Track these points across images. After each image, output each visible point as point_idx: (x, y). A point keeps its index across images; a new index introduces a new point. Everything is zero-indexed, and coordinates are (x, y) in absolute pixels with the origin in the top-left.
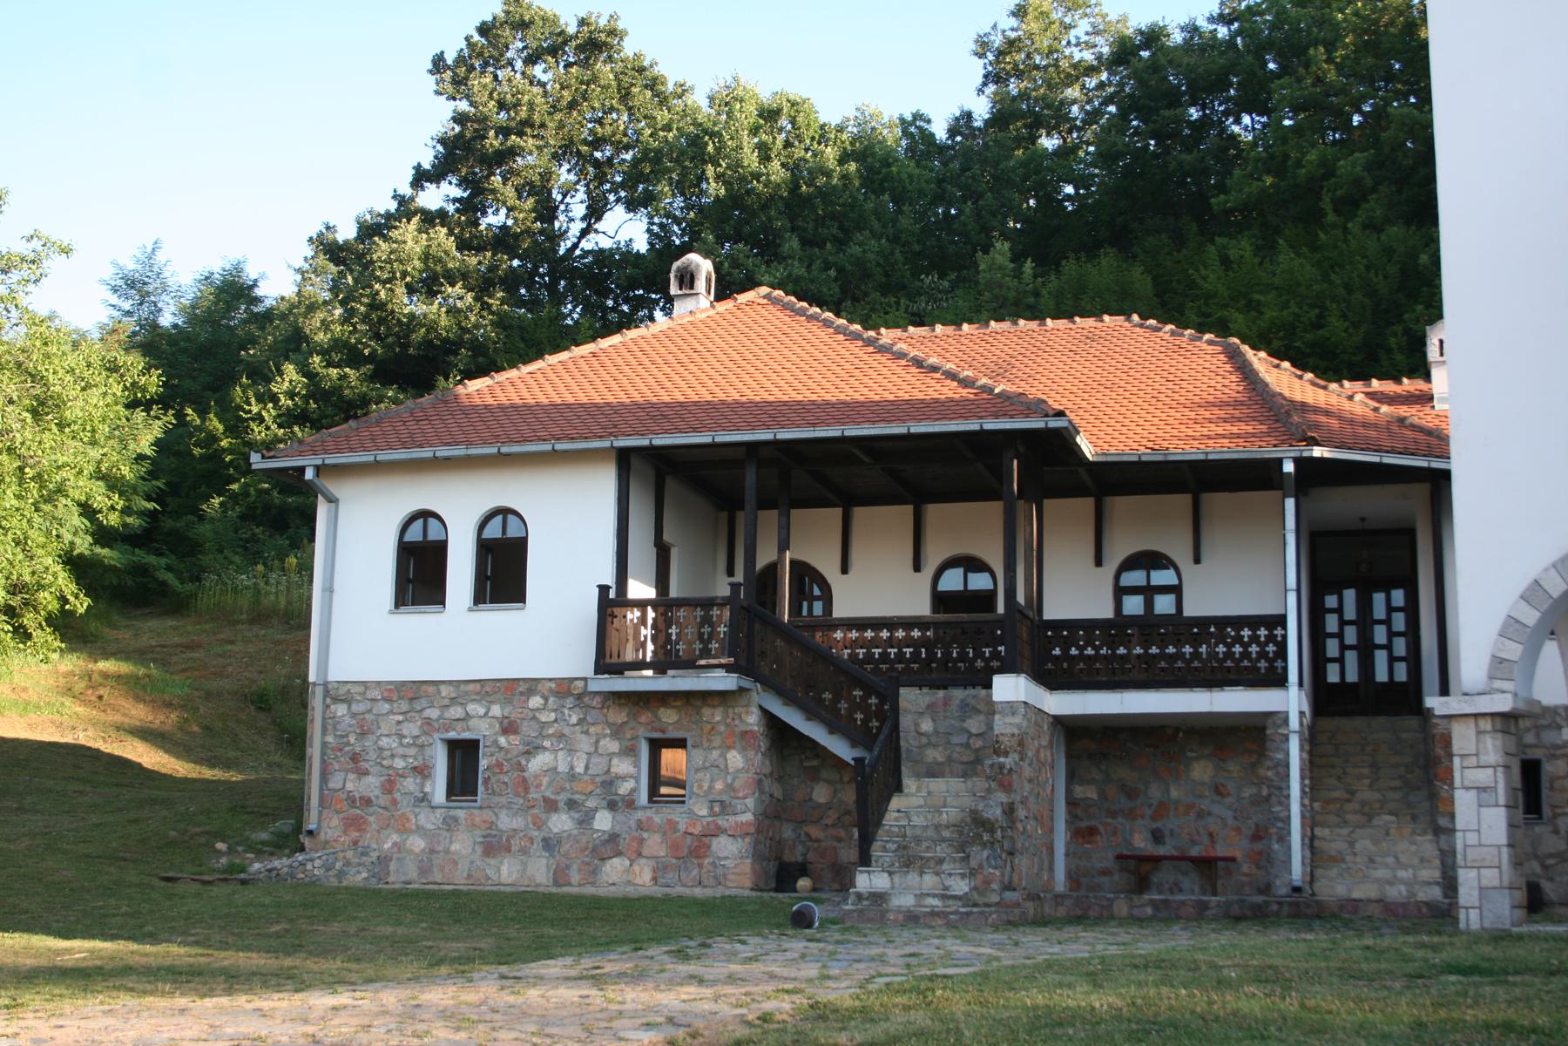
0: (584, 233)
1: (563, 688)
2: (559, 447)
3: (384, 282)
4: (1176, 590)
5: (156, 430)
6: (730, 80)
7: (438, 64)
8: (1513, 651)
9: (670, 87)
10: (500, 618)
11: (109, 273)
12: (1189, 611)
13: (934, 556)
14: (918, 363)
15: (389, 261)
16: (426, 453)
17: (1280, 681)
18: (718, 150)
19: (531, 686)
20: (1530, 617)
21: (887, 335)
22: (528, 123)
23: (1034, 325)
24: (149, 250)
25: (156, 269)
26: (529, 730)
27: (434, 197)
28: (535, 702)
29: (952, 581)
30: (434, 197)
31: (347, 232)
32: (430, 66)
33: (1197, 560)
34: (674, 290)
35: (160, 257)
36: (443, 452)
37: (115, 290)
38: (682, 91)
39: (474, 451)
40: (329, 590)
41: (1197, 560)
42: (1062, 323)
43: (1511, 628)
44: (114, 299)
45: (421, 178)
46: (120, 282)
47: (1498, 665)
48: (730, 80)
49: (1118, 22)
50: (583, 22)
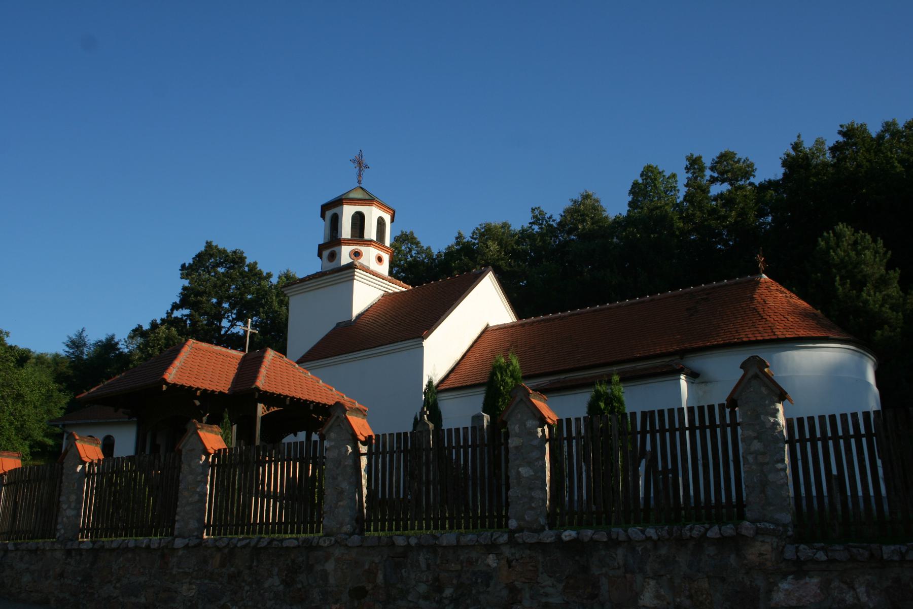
0: (232, 326)
2: (120, 420)
3: (151, 347)
5: (67, 399)
6: (286, 271)
7: (183, 267)
9: (265, 274)
11: (66, 340)
15: (154, 340)
16: (88, 421)
18: (266, 302)
22: (205, 292)
24: (80, 332)
25: (82, 338)
27: (177, 314)
30: (177, 314)
31: (146, 327)
32: (180, 268)
35: (84, 334)
36: (93, 421)
37: (68, 346)
38: (269, 275)
39: (101, 421)
44: (67, 349)
45: (175, 307)
46: (69, 343)
48: (286, 271)
49: (427, 249)
50: (235, 252)
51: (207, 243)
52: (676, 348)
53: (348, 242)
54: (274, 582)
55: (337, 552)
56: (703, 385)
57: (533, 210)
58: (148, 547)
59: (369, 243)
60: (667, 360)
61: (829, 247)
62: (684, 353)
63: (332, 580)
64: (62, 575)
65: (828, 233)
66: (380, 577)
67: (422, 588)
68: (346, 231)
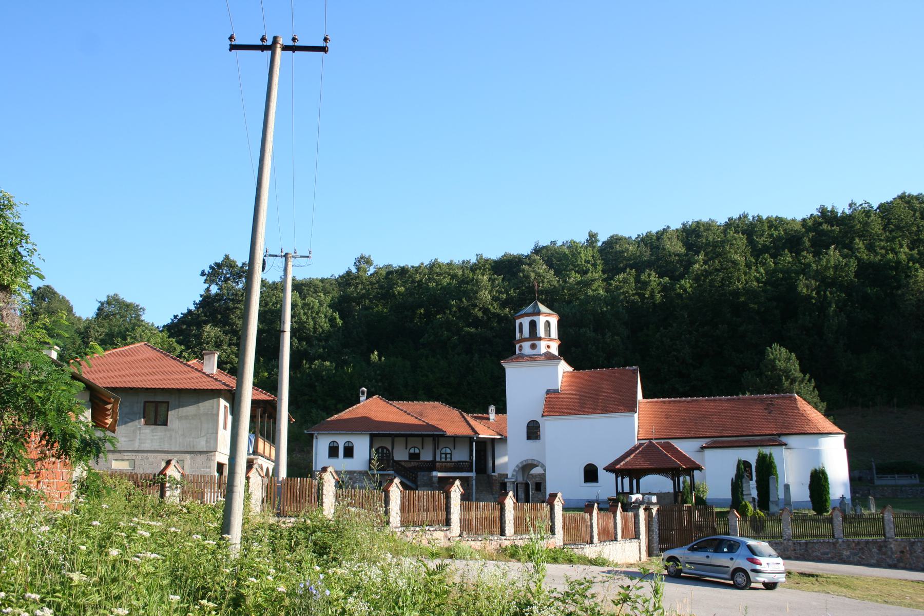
1: (360, 472)
4: (451, 454)
7: (203, 274)
8: (515, 474)
10: (348, 460)
12: (454, 460)
13: (409, 447)
14: (398, 408)
17: (471, 471)
19: (355, 472)
20: (517, 469)
21: (395, 403)
23: (422, 402)
26: (354, 479)
28: (355, 474)
29: (412, 451)
33: (454, 449)
34: (360, 395)
40: (316, 454)
41: (454, 449)
42: (427, 402)
43: (515, 470)
47: (513, 475)
51: (226, 255)
52: (774, 432)
53: (545, 340)
54: (875, 550)
55: (894, 542)
56: (788, 450)
57: (477, 255)
58: (828, 542)
59: (553, 340)
60: (771, 437)
61: (775, 359)
62: (780, 435)
63: (894, 549)
64: (795, 550)
65: (771, 348)
66: (908, 548)
67: (920, 551)
68: (541, 332)
